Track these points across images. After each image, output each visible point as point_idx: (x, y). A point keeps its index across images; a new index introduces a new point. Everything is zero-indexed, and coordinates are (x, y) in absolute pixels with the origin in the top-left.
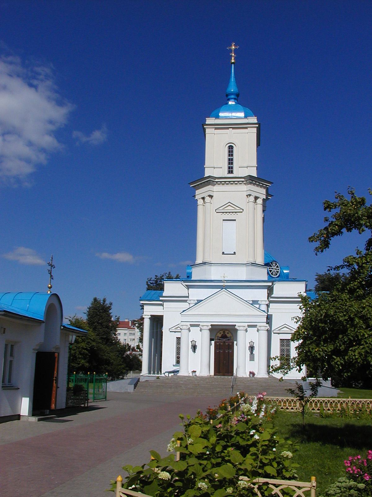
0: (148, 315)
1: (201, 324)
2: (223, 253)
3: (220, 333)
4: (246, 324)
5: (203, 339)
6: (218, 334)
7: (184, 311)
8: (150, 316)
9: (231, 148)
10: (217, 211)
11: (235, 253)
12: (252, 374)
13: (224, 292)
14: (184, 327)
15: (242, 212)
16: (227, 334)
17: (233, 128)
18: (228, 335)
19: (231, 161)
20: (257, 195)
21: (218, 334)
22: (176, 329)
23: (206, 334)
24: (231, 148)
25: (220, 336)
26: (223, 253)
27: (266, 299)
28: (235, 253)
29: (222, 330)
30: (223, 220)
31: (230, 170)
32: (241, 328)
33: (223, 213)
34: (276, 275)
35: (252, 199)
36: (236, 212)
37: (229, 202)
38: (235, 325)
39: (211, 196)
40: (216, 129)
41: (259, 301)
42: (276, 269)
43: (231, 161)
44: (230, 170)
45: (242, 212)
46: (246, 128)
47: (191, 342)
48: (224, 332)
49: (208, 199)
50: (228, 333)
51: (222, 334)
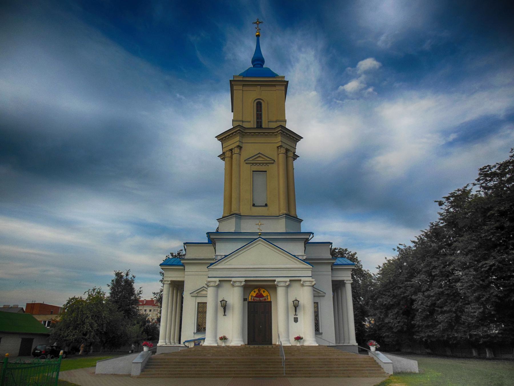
0: (168, 281)
2: (254, 205)
3: (255, 292)
4: (288, 279)
5: (234, 297)
8: (169, 282)
9: (259, 106)
11: (266, 205)
13: (260, 242)
15: (273, 163)
16: (262, 293)
17: (261, 85)
18: (265, 294)
19: (259, 116)
21: (252, 292)
22: (198, 293)
24: (259, 106)
25: (255, 295)
26: (254, 205)
27: (303, 254)
32: (282, 284)
33: (253, 164)
35: (283, 150)
36: (266, 163)
38: (275, 281)
45: (273, 163)
46: (275, 85)
47: (221, 301)
48: (259, 291)
50: (264, 292)
51: (256, 292)
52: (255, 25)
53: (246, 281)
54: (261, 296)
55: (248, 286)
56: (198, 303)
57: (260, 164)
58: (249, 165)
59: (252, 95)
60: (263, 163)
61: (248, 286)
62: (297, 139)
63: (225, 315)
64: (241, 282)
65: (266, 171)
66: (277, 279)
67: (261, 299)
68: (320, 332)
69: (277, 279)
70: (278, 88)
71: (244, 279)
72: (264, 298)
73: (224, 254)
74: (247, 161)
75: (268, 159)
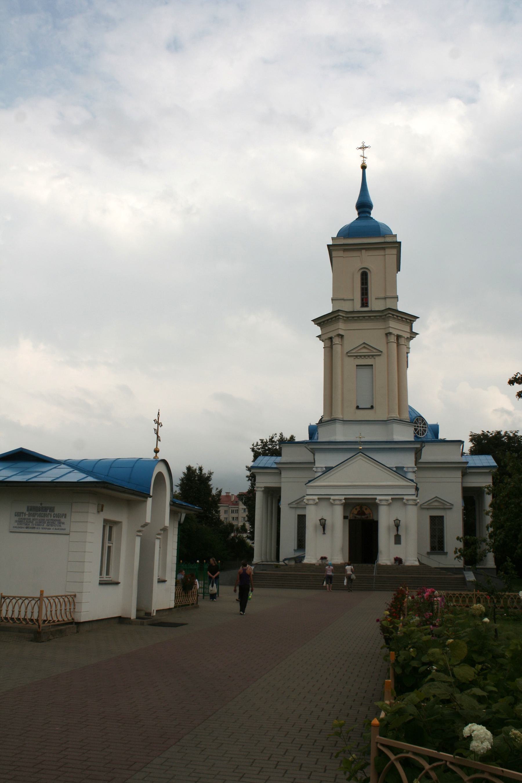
0: (261, 488)
1: (332, 497)
2: (358, 407)
3: (356, 509)
4: (389, 498)
6: (354, 510)
7: (310, 481)
8: (263, 489)
9: (364, 276)
10: (349, 354)
11: (372, 407)
12: (398, 560)
14: (311, 502)
16: (365, 511)
18: (367, 512)
19: (365, 292)
20: (400, 333)
21: (354, 510)
23: (339, 511)
24: (364, 276)
27: (414, 465)
28: (372, 407)
29: (358, 504)
30: (357, 365)
31: (365, 303)
33: (356, 356)
34: (423, 434)
35: (393, 339)
36: (373, 356)
37: (364, 343)
38: (376, 499)
39: (341, 336)
40: (345, 250)
41: (404, 467)
42: (423, 427)
43: (365, 292)
44: (365, 303)
45: (380, 355)
46: (384, 249)
47: (320, 520)
48: (361, 507)
49: (336, 340)
50: (366, 509)
51: (358, 510)
52: (361, 151)
53: (345, 499)
54: (363, 513)
55: (349, 504)
56: (299, 516)
57: (365, 356)
58: (352, 358)
59: (356, 262)
60: (369, 356)
61: (349, 504)
62: (411, 320)
63: (324, 533)
64: (341, 500)
65: (372, 365)
66: (379, 498)
67: (363, 517)
68: (445, 551)
69: (379, 498)
70: (388, 251)
71: (343, 497)
72: (366, 516)
73: (324, 466)
74: (349, 354)
75: (375, 351)
